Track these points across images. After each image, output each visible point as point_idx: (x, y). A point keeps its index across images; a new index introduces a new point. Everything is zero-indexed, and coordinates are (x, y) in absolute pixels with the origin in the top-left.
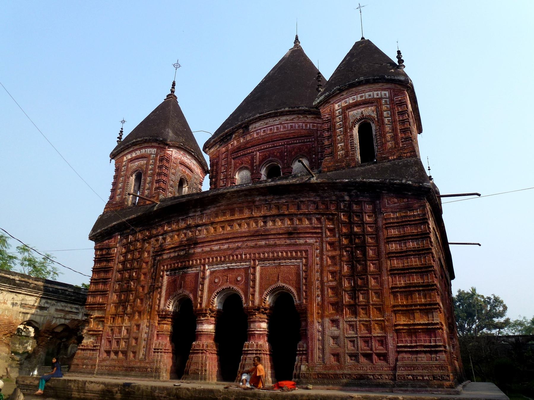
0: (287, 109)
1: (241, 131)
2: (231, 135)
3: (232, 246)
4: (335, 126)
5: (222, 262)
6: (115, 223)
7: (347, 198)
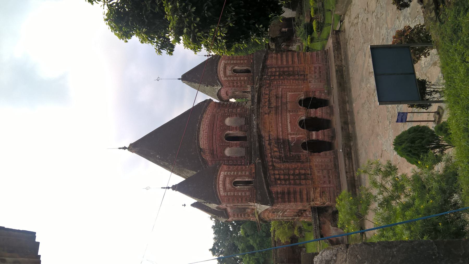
0: (197, 125)
1: (202, 153)
2: (203, 159)
3: (280, 122)
4: (232, 80)
5: (287, 126)
6: (265, 187)
7: (265, 77)
